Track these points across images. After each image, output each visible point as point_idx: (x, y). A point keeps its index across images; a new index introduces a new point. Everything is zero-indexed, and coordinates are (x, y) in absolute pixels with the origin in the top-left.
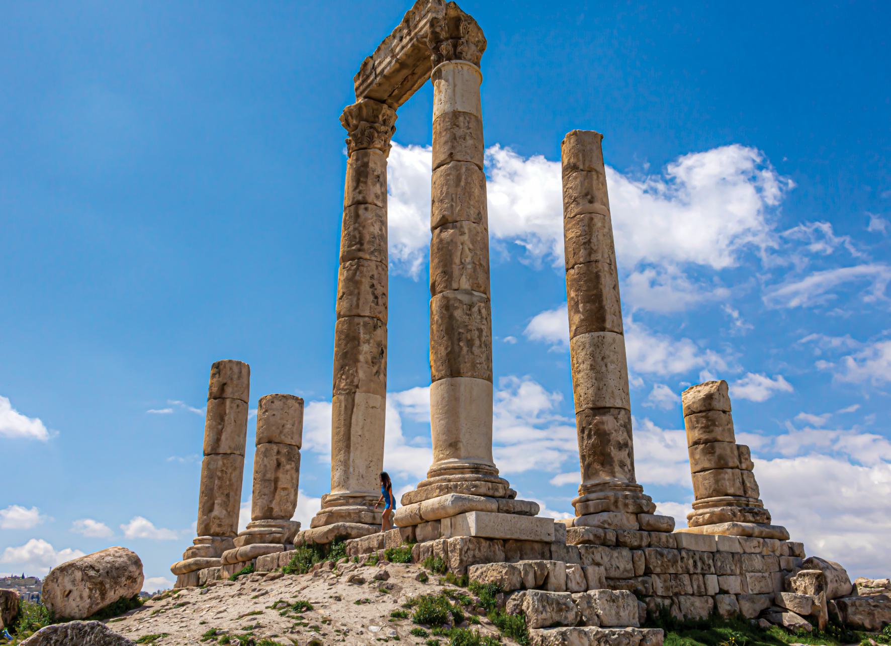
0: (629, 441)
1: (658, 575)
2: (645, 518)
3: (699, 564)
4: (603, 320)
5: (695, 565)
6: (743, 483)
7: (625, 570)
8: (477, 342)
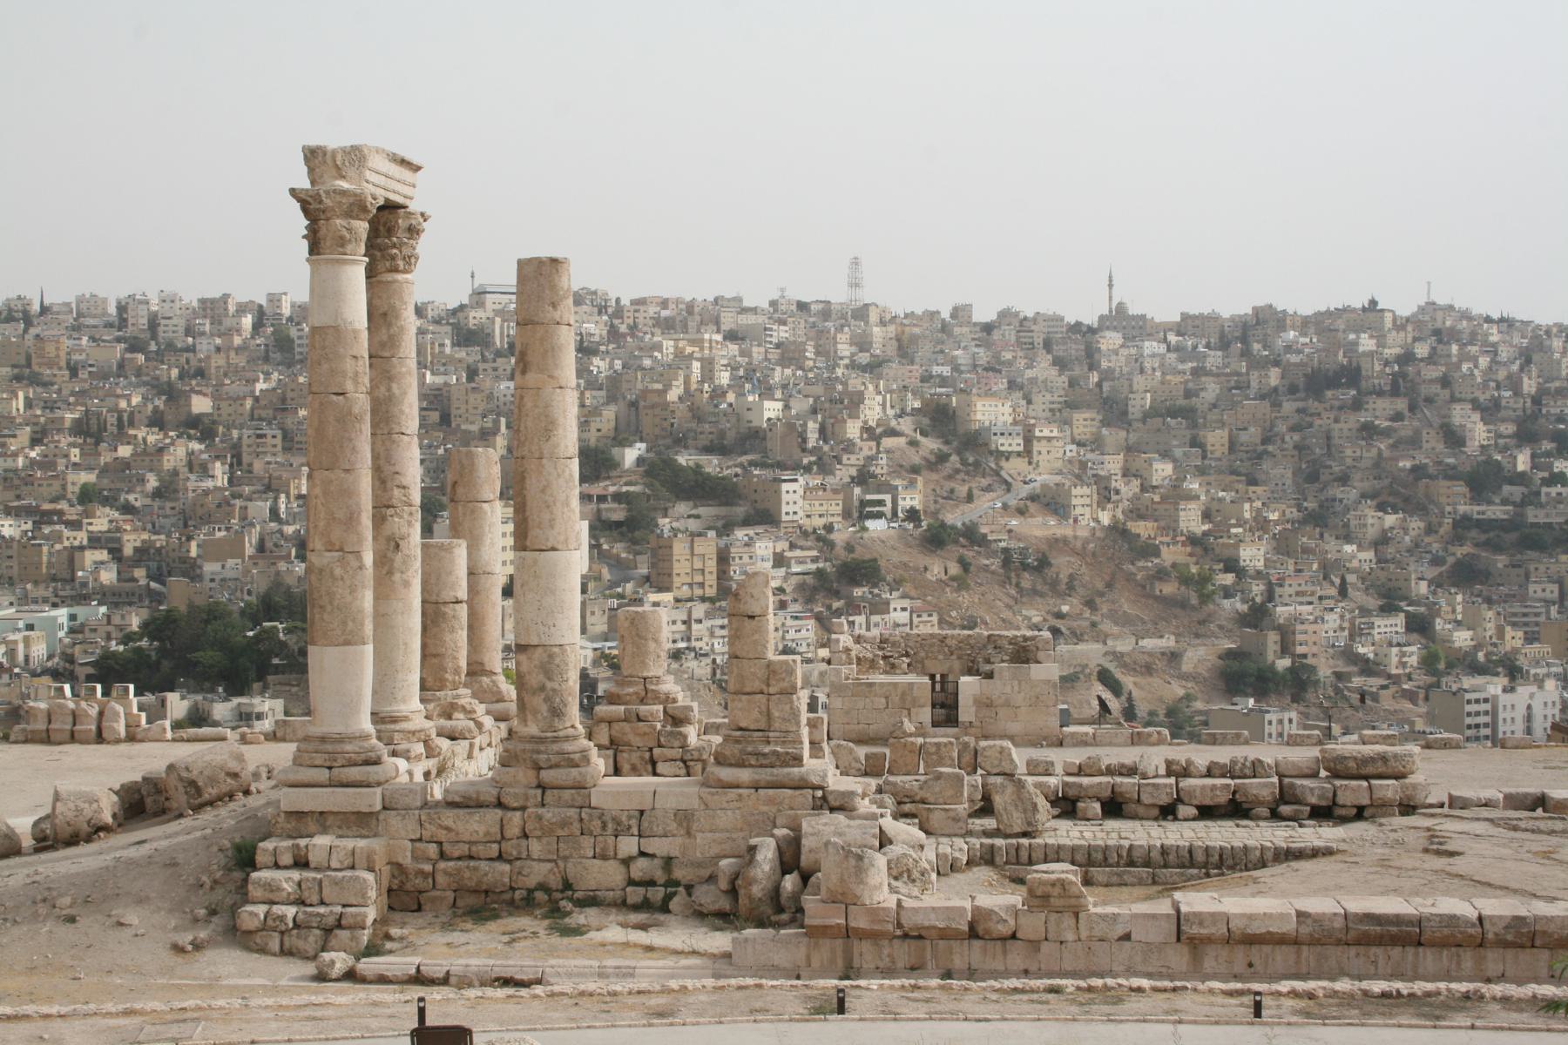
0: (549, 685)
1: (538, 838)
2: (543, 773)
3: (610, 825)
4: (526, 537)
5: (604, 827)
6: (769, 715)
7: (487, 833)
8: (329, 608)
